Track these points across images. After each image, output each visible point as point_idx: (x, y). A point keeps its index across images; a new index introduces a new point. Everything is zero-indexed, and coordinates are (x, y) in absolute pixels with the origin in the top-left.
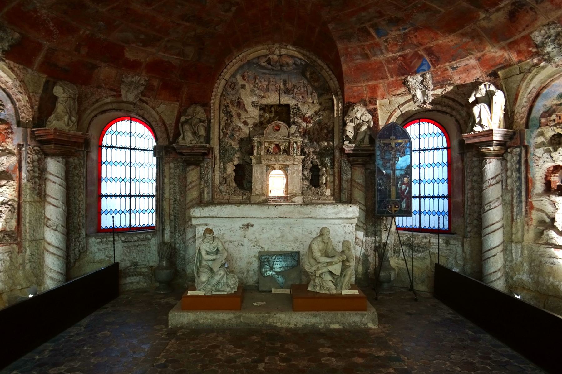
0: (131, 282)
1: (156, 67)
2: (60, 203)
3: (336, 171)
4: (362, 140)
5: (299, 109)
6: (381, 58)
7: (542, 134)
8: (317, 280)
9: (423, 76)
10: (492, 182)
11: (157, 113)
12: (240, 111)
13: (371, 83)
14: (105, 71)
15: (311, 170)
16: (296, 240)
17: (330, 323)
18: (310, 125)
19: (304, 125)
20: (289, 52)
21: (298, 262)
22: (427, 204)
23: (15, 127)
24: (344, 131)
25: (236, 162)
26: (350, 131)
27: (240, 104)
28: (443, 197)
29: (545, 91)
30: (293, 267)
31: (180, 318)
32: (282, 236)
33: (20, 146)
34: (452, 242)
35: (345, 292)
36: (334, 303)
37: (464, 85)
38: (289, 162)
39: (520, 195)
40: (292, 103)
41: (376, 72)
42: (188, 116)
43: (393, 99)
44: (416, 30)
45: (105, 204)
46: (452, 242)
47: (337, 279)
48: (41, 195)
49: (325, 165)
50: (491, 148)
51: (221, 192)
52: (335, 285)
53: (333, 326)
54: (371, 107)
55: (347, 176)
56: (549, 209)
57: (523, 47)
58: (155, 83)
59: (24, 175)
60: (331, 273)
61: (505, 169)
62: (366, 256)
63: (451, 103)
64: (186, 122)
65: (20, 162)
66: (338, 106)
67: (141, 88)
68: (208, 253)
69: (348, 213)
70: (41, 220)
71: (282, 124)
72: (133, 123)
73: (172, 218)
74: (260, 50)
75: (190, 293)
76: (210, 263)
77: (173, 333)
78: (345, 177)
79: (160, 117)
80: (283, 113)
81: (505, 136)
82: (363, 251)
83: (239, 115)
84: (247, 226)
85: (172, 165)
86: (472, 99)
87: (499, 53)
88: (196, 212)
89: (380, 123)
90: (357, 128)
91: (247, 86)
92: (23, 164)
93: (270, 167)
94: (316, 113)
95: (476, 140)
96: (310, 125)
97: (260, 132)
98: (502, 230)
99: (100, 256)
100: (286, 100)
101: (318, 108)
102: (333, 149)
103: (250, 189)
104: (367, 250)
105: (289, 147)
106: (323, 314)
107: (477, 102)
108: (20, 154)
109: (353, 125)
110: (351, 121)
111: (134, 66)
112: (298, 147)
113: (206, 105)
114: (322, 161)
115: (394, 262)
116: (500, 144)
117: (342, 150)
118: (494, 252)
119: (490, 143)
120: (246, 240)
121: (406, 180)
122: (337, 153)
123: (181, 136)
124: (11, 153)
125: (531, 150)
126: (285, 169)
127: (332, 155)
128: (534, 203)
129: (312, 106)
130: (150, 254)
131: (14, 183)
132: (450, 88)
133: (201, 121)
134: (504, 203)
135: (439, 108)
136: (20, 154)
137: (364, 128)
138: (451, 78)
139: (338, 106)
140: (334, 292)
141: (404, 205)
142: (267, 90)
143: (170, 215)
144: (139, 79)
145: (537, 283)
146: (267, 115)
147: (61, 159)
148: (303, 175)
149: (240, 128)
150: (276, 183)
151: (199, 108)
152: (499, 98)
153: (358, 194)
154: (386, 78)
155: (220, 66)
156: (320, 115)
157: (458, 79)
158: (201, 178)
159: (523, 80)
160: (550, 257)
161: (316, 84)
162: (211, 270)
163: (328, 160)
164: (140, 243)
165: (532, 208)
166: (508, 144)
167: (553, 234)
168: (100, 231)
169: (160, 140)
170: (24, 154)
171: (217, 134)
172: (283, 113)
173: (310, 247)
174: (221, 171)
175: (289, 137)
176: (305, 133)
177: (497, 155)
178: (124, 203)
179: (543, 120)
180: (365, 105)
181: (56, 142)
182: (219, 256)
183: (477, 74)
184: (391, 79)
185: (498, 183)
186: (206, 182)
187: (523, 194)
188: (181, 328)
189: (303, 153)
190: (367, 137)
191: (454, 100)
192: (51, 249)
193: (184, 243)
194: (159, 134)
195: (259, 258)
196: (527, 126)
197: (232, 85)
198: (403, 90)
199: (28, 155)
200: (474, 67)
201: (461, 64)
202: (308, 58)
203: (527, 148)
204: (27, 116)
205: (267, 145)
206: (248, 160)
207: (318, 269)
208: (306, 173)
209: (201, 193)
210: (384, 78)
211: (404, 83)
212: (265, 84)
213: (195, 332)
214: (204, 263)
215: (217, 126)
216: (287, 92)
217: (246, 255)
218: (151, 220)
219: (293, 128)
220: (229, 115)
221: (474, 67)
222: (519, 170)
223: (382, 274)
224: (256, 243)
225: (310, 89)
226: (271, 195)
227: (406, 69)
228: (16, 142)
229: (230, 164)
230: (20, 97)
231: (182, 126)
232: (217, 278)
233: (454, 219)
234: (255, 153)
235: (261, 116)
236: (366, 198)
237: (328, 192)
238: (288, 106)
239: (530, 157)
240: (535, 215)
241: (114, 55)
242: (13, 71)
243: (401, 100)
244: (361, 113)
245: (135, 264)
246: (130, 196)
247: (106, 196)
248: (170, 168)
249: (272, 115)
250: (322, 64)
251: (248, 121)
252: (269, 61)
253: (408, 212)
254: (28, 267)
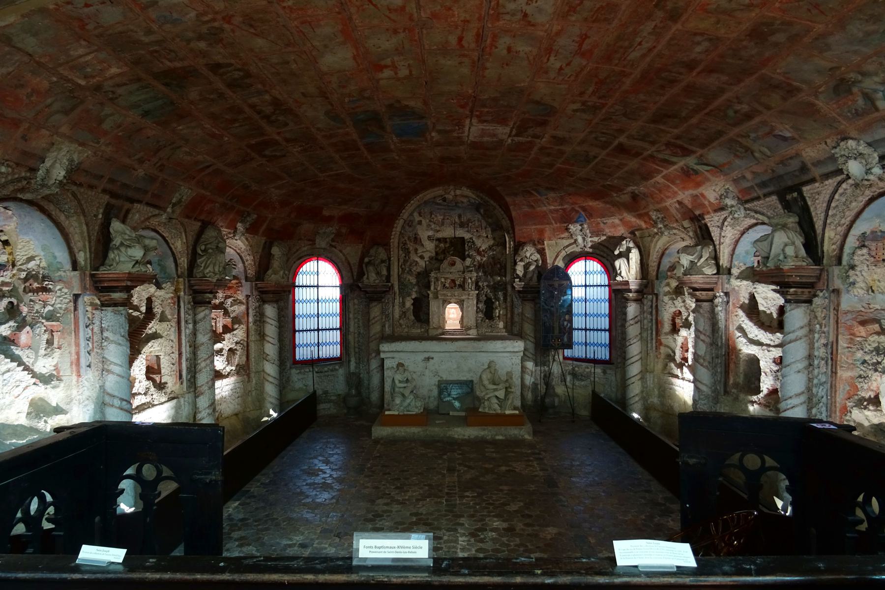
0: (325, 409)
1: (346, 219)
2: (276, 341)
3: (508, 305)
4: (531, 279)
5: (473, 242)
6: (545, 208)
7: (668, 285)
8: (486, 403)
9: (581, 225)
10: (631, 322)
11: (344, 255)
12: (417, 247)
13: (538, 227)
14: (307, 226)
15: (486, 303)
16: (470, 370)
17: (496, 435)
18: (484, 259)
19: (478, 258)
20: (466, 193)
21: (472, 389)
22: (593, 337)
23: (243, 281)
24: (515, 270)
25: (413, 297)
26: (520, 270)
27: (417, 240)
28: (605, 330)
29: (667, 252)
30: (468, 393)
31: (380, 431)
32: (458, 367)
33: (248, 297)
34: (608, 371)
35: (507, 412)
36: (500, 420)
37: (614, 237)
38: (463, 298)
39: (652, 333)
40: (467, 236)
41: (542, 219)
42: (371, 256)
43: (559, 241)
44: (570, 195)
45: (300, 338)
46: (608, 371)
47: (501, 402)
48: (262, 336)
49: (498, 299)
50: (631, 295)
51: (401, 325)
52: (500, 406)
53: (498, 437)
54: (539, 246)
55: (518, 310)
56: (672, 345)
57: (646, 219)
58: (344, 230)
59: (251, 319)
60: (497, 397)
61: (642, 312)
62: (535, 385)
63: (605, 250)
64: (369, 263)
65: (248, 309)
66: (510, 244)
67: (332, 236)
68: (400, 382)
69: (514, 347)
70: (263, 356)
71: (458, 260)
72: (320, 262)
73: (357, 350)
74: (438, 191)
75: (387, 413)
76: (401, 390)
77: (377, 441)
78: (516, 311)
79: (346, 259)
80: (458, 248)
81: (640, 285)
82: (533, 380)
83: (416, 250)
84: (428, 359)
85: (356, 301)
86: (617, 252)
87: (633, 219)
88: (385, 347)
89: (548, 261)
90: (526, 267)
91: (423, 222)
92: (250, 311)
93: (446, 302)
94: (490, 248)
95: (619, 287)
96: (484, 259)
97: (436, 266)
98: (640, 362)
99: (299, 385)
100: (461, 233)
101: (491, 242)
102: (506, 284)
103: (427, 321)
104: (536, 379)
105: (464, 282)
106: (490, 428)
107: (620, 255)
108: (247, 303)
109: (523, 264)
110: (521, 260)
111: (328, 220)
112: (472, 282)
113: (386, 245)
114: (495, 295)
115: (560, 390)
116: (637, 291)
117: (513, 287)
118: (633, 380)
119: (630, 291)
120: (427, 371)
121: (567, 317)
122: (509, 288)
123: (366, 276)
124: (241, 303)
125: (661, 297)
126: (461, 303)
127: (505, 289)
128: (663, 340)
129: (486, 240)
130: (338, 384)
131: (244, 326)
132: (604, 238)
133: (383, 261)
134: (641, 339)
135: (598, 252)
136: (247, 303)
137: (532, 268)
138: (603, 231)
139: (510, 244)
140: (499, 412)
141: (566, 339)
142: (443, 224)
143: (355, 347)
144: (332, 230)
145: (663, 404)
146: (442, 245)
147: (275, 305)
148: (478, 308)
150: (452, 315)
151: (381, 250)
152: (635, 255)
153: (528, 328)
154: (552, 224)
155: (401, 207)
156: (494, 250)
157: (610, 232)
158: (382, 313)
159: (652, 241)
160: (672, 384)
161: (490, 220)
162: (403, 395)
163: (500, 294)
164: (330, 373)
165: (661, 344)
166: (645, 291)
167: (672, 365)
168: (296, 362)
169: (346, 278)
170: (250, 303)
171: (396, 270)
172: (458, 248)
173: (481, 377)
174: (400, 306)
175: (464, 272)
176: (480, 266)
177: (636, 300)
178: (311, 337)
179: (669, 273)
180: (534, 245)
181: (274, 292)
182: (409, 384)
183: (621, 231)
184: (555, 225)
185: (636, 323)
186: (387, 316)
187: (654, 333)
188: (382, 438)
189: (477, 287)
190: (535, 276)
191: (607, 248)
192: (270, 379)
193: (368, 373)
194: (344, 273)
195: (439, 386)
196: (657, 278)
197: (409, 223)
199: (253, 304)
200: (618, 225)
201: (610, 221)
202: (482, 199)
203: (657, 295)
204: (251, 272)
205: (443, 280)
206: (425, 293)
207: (487, 394)
208: (480, 306)
209: (384, 326)
210: (550, 223)
211: (567, 229)
212: (440, 218)
213: (392, 442)
214: (397, 389)
215: (396, 264)
216: (462, 225)
217: (428, 383)
218: (334, 351)
219: (468, 261)
220: (407, 252)
221: (618, 225)
222: (651, 313)
223: (547, 400)
224: (436, 373)
225: (484, 224)
226: (447, 328)
227: (567, 219)
228: (245, 293)
229: (409, 298)
230: (248, 257)
231: (366, 267)
232: (408, 401)
233: (613, 351)
234: (432, 288)
235: (436, 246)
236: (536, 331)
237: (501, 325)
238: (462, 239)
239: (660, 302)
240: (663, 350)
241: (315, 215)
242: (247, 239)
243: (566, 242)
244: (530, 253)
245: (326, 393)
246: (318, 330)
247: (299, 331)
248: (354, 304)
249: (448, 245)
250: (495, 204)
251: (424, 255)
252: (444, 200)
253: (570, 346)
254: (254, 393)
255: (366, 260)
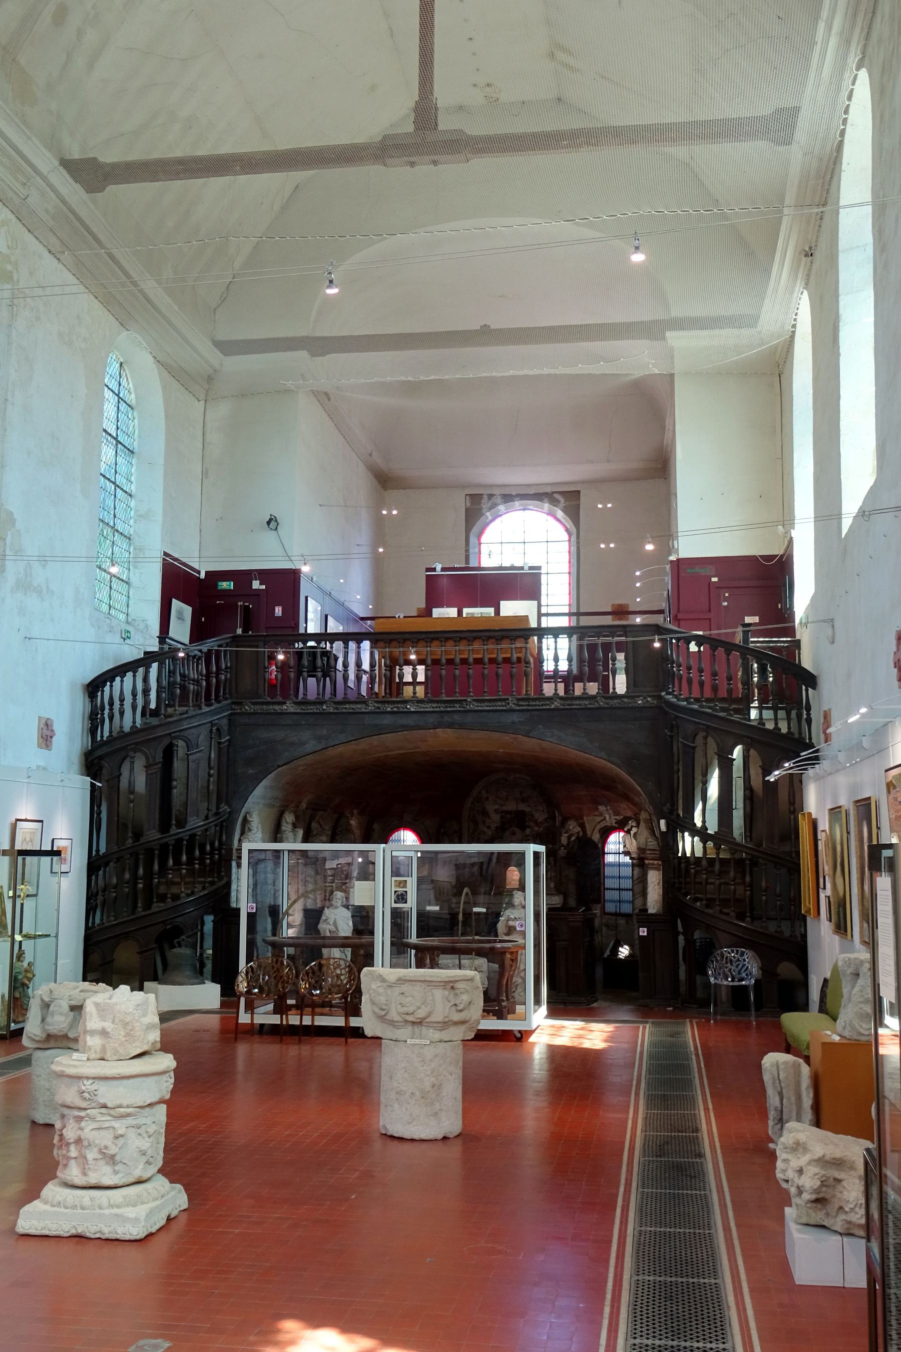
5: (532, 816)
19: (536, 828)
26: (564, 840)
27: (485, 813)
40: (527, 809)
66: (558, 819)
71: (517, 830)
83: (484, 822)
90: (569, 838)
94: (546, 820)
100: (522, 807)
101: (546, 816)
110: (566, 832)
137: (573, 838)
139: (558, 819)
146: (508, 816)
149: (484, 833)
180: (577, 820)
198: (597, 813)
211: (597, 809)
216: (523, 800)
219: (528, 831)
235: (502, 817)
238: (523, 812)
243: (599, 819)
244: (573, 827)
255: (442, 831)
